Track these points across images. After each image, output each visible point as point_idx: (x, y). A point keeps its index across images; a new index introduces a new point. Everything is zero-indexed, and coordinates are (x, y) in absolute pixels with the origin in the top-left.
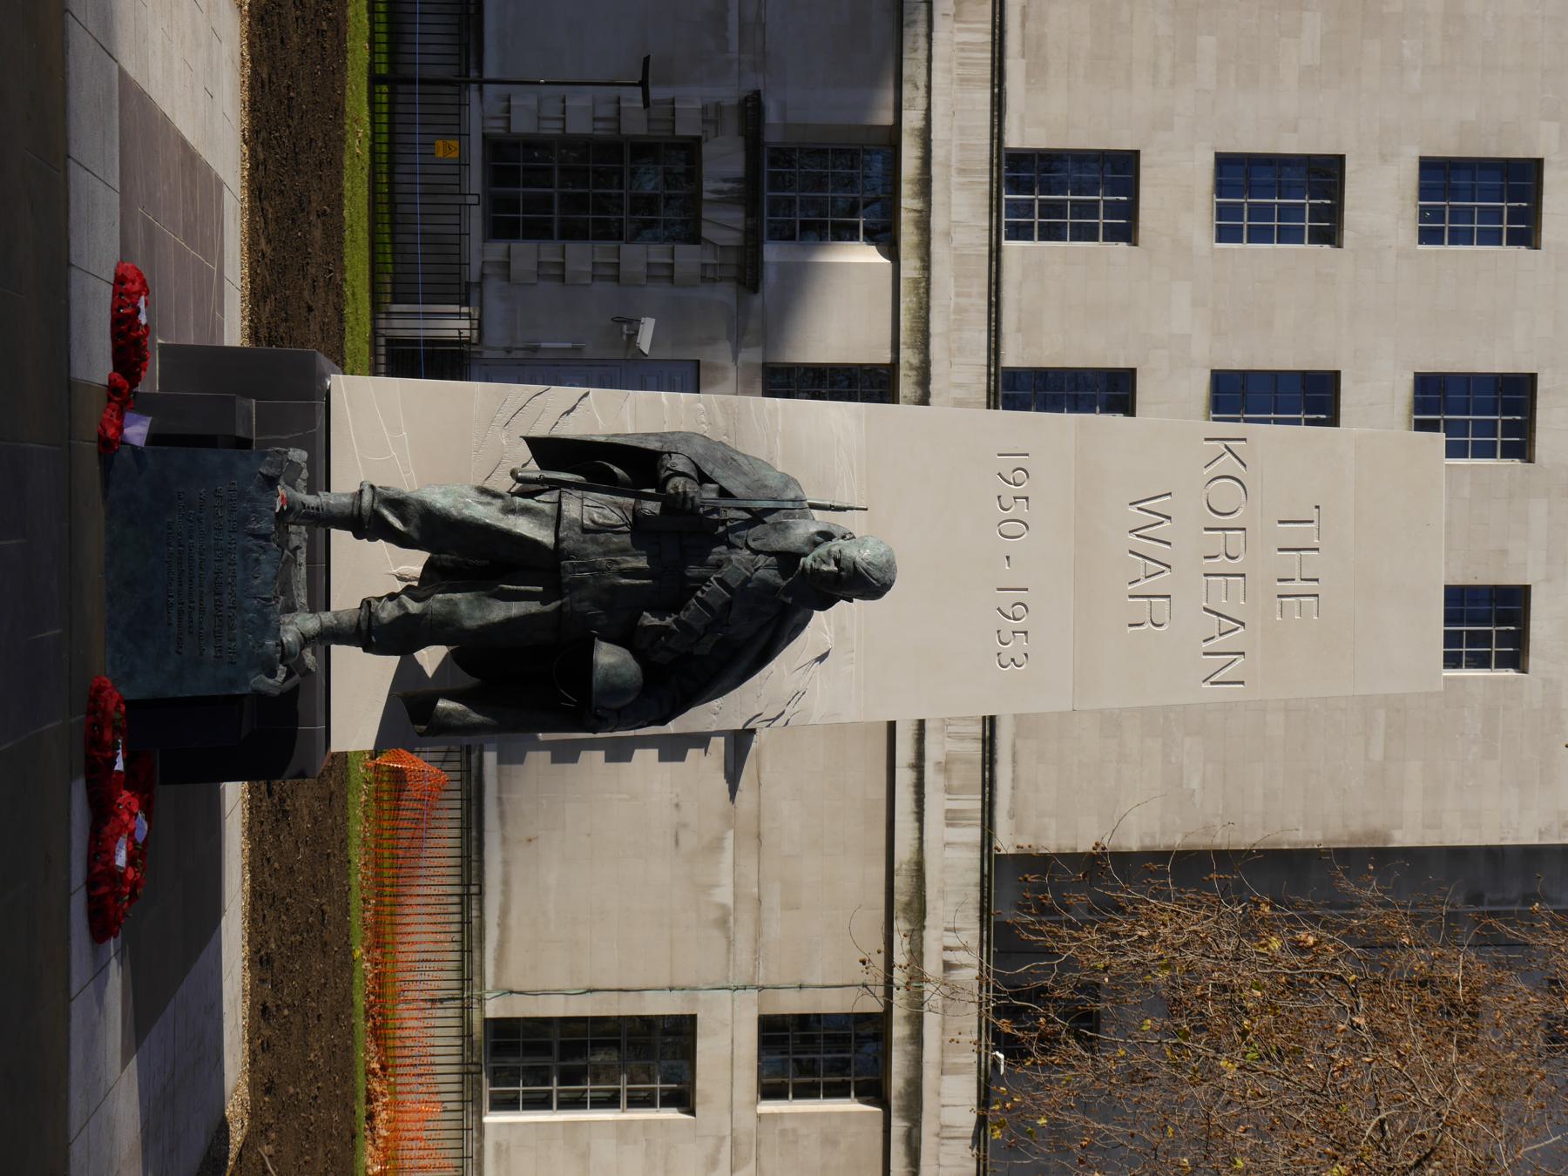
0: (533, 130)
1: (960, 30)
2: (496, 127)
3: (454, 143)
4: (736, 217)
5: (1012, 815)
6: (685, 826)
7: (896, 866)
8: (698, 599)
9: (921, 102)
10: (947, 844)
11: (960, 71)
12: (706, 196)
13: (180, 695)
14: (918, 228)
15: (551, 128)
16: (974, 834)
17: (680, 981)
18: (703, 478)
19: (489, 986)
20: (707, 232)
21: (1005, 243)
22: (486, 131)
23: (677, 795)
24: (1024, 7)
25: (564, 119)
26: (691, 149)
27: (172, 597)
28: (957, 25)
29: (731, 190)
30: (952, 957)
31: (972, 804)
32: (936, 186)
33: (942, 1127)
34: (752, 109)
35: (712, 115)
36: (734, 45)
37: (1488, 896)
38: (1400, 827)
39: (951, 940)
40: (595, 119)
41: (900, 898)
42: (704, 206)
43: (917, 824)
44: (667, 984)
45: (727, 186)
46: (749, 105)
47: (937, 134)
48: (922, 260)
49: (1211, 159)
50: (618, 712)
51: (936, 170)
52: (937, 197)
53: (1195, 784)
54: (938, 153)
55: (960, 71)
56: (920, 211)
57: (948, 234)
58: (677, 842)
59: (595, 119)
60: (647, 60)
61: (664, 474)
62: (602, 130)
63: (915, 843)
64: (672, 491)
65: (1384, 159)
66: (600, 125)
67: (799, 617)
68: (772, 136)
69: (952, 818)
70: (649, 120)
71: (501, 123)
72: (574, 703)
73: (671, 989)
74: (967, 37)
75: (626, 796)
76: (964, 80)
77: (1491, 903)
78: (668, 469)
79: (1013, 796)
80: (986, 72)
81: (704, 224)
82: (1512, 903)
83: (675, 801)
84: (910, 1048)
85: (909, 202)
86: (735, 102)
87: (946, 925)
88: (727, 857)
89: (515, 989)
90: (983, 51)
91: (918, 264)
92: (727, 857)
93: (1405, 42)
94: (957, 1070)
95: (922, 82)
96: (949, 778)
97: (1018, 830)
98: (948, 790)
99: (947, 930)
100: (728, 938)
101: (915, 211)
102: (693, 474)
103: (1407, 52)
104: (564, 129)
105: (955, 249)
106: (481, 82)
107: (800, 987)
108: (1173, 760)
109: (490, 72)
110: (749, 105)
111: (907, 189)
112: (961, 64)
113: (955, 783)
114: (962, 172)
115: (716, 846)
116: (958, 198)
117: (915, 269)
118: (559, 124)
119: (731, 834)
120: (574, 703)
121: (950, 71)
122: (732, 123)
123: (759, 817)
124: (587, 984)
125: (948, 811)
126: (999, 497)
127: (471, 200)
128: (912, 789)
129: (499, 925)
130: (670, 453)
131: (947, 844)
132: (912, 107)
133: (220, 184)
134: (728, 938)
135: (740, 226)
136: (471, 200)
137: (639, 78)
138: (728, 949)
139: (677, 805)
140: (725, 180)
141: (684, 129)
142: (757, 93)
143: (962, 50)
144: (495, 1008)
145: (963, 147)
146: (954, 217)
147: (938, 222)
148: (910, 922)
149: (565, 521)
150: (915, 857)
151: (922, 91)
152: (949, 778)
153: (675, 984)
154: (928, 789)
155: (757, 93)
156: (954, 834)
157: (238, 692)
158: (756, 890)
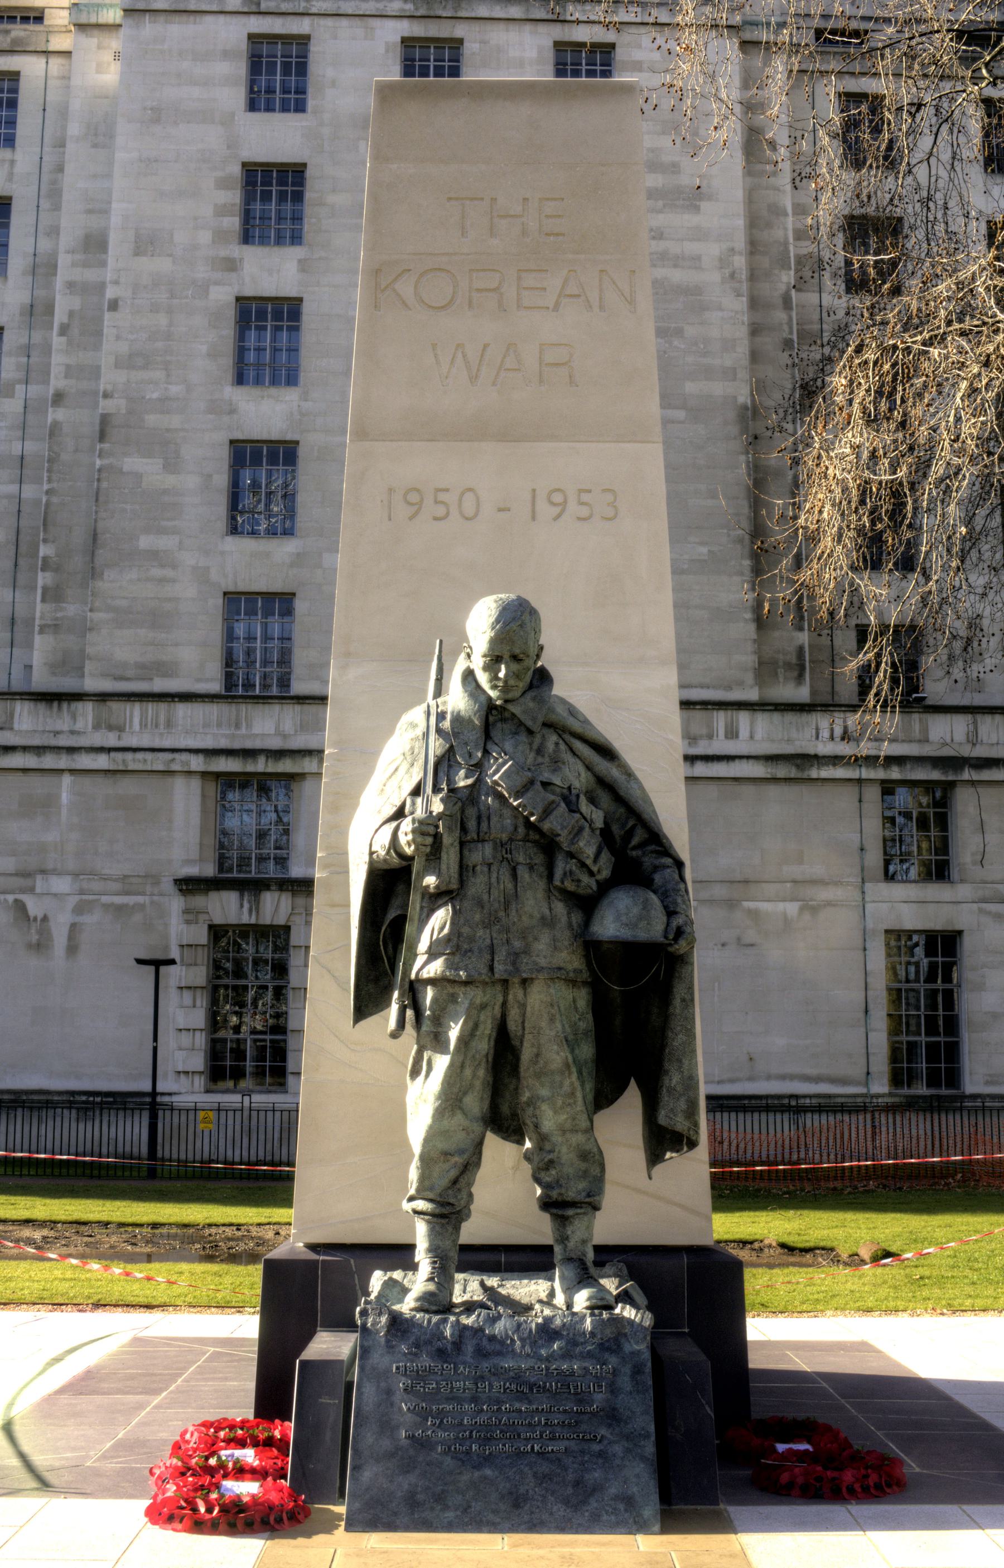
0: (202, 1054)
1: (131, 727)
2: (199, 1082)
3: (201, 1115)
4: (269, 898)
5: (729, 688)
6: (739, 939)
7: (769, 776)
8: (541, 819)
9: (184, 757)
10: (752, 737)
11: (162, 727)
12: (253, 921)
13: (653, 1438)
14: (280, 759)
15: (201, 1040)
16: (743, 718)
17: (860, 941)
18: (399, 814)
19: (861, 1090)
20: (281, 920)
21: (292, 694)
22: (202, 1090)
23: (716, 945)
24: (115, 679)
25: (194, 1030)
26: (217, 932)
27: (533, 1448)
28: (127, 729)
29: (249, 902)
30: (838, 731)
31: (720, 719)
32: (249, 745)
33: (968, 741)
34: (188, 885)
35: (190, 915)
36: (140, 899)
37: (786, 335)
38: (735, 398)
39: (825, 734)
40: (194, 1006)
41: (793, 773)
42: (261, 922)
43: (737, 761)
44: (861, 952)
45: (246, 905)
46: (184, 887)
47: (209, 743)
48: (304, 756)
49: (229, 539)
50: (671, 913)
51: (237, 745)
52: (258, 744)
53: (704, 550)
54: (223, 743)
55: (162, 727)
56: (267, 757)
57: (285, 737)
58: (752, 945)
59: (194, 1006)
60: (140, 961)
61: (396, 861)
62: (202, 1001)
63: (751, 762)
64: (413, 848)
65: (232, 411)
66: (198, 1003)
67: (560, 709)
68: (209, 870)
69: (732, 734)
70: (196, 965)
71: (197, 1078)
72: (659, 968)
73: (865, 949)
74: (136, 720)
75: (716, 984)
76: (169, 724)
77: (791, 333)
78: (388, 853)
79: (715, 687)
80: (163, 707)
81: (275, 923)
82: (790, 319)
83: (720, 947)
84: (908, 766)
85: (261, 765)
86: (182, 899)
87: (814, 739)
88: (765, 906)
89: (865, 1070)
90: (147, 710)
91: (307, 760)
92: (765, 906)
93: (148, 397)
94: (925, 730)
95: (168, 756)
96: (701, 737)
97: (740, 684)
98: (710, 737)
99: (817, 738)
100: (825, 905)
101: (267, 761)
102: (394, 824)
103: (155, 396)
104: (201, 1030)
105: (296, 731)
106: (154, 1093)
107: (862, 850)
108: (686, 566)
109: (146, 1086)
110: (184, 887)
111: (250, 768)
112: (157, 726)
113: (704, 731)
114: (237, 726)
115: (755, 915)
116: (257, 730)
117: (311, 762)
118: (198, 1034)
119: (746, 904)
120: (659, 968)
121: (161, 734)
122: (199, 901)
123: (732, 882)
124: (862, 1015)
125: (726, 737)
126: (436, 519)
127: (246, 1103)
128: (710, 764)
129: (817, 1083)
130: (371, 853)
131: (752, 737)
132: (188, 763)
133: (137, 1341)
134: (825, 905)
135: (276, 894)
136: (246, 1103)
137: (152, 969)
138: (834, 905)
139: (723, 945)
140: (242, 906)
141: (201, 935)
142: (176, 881)
143: (146, 725)
144: (880, 1087)
145: (219, 725)
146: (272, 732)
147: (275, 743)
148: (812, 766)
149: (448, 974)
150: (762, 762)
151: (177, 756)
152: (701, 737)
153: (861, 946)
154: (710, 752)
155: (176, 881)
156: (744, 732)
157: (649, 1364)
158: (788, 885)
